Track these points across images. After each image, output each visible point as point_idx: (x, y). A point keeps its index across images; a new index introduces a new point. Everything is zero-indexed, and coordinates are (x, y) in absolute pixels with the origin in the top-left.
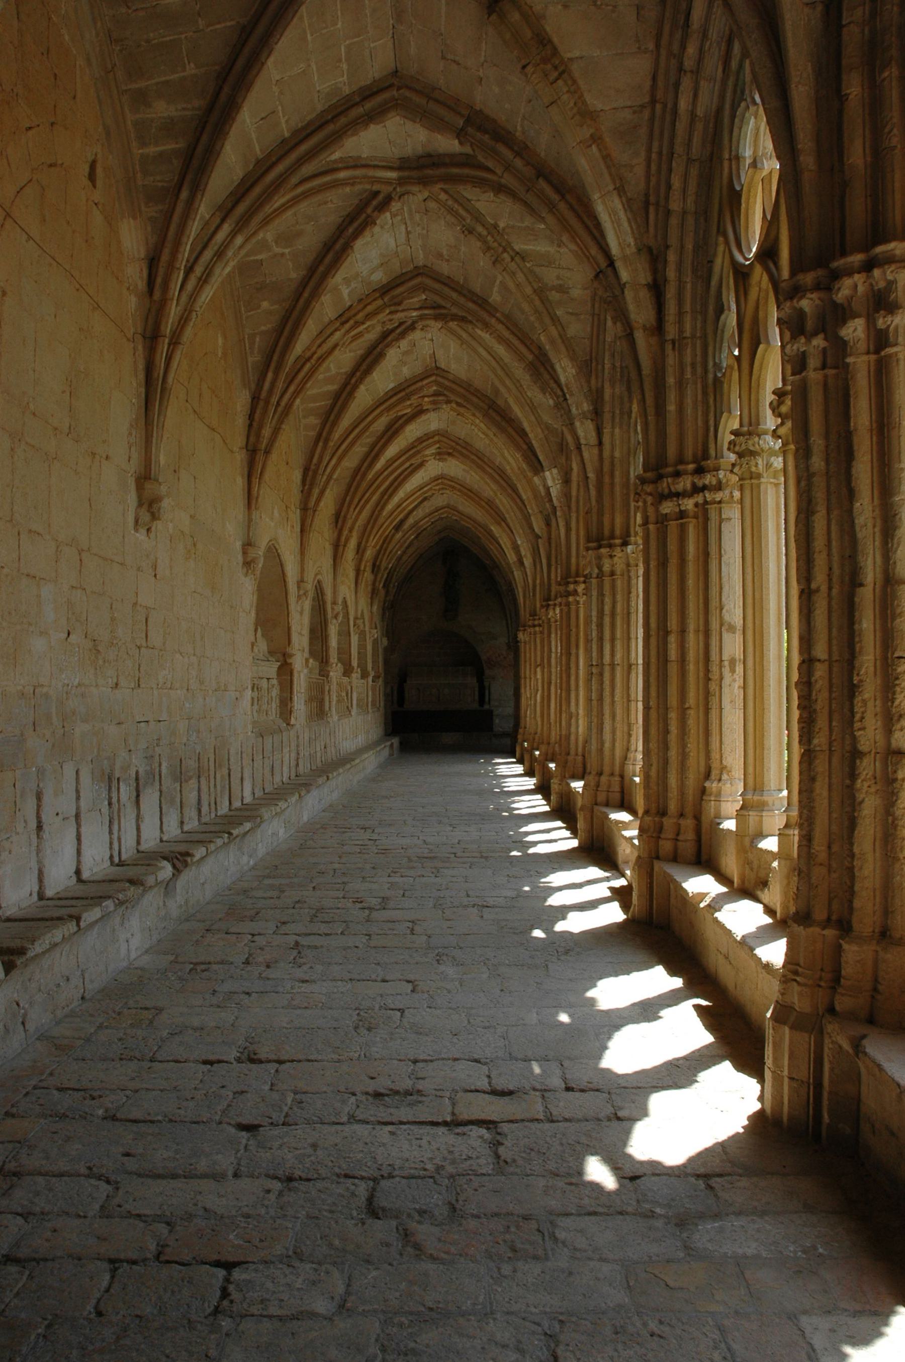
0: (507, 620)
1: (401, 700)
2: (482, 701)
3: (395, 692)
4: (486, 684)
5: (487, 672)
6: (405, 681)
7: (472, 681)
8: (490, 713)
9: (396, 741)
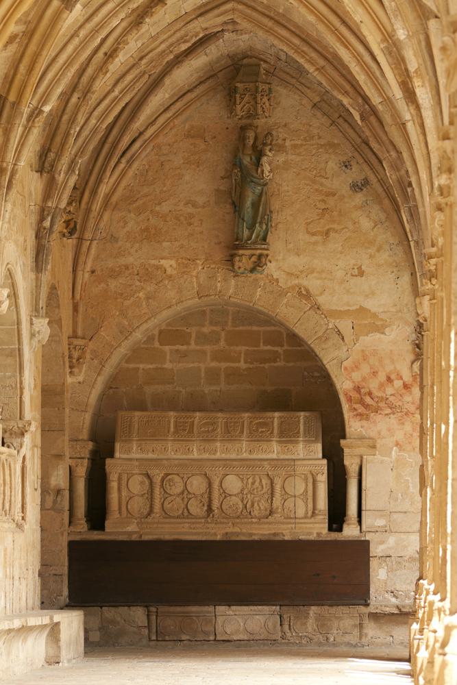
1: (97, 513)
2: (337, 517)
4: (351, 463)
5: (353, 426)
6: (112, 456)
8: (361, 549)
9: (71, 623)
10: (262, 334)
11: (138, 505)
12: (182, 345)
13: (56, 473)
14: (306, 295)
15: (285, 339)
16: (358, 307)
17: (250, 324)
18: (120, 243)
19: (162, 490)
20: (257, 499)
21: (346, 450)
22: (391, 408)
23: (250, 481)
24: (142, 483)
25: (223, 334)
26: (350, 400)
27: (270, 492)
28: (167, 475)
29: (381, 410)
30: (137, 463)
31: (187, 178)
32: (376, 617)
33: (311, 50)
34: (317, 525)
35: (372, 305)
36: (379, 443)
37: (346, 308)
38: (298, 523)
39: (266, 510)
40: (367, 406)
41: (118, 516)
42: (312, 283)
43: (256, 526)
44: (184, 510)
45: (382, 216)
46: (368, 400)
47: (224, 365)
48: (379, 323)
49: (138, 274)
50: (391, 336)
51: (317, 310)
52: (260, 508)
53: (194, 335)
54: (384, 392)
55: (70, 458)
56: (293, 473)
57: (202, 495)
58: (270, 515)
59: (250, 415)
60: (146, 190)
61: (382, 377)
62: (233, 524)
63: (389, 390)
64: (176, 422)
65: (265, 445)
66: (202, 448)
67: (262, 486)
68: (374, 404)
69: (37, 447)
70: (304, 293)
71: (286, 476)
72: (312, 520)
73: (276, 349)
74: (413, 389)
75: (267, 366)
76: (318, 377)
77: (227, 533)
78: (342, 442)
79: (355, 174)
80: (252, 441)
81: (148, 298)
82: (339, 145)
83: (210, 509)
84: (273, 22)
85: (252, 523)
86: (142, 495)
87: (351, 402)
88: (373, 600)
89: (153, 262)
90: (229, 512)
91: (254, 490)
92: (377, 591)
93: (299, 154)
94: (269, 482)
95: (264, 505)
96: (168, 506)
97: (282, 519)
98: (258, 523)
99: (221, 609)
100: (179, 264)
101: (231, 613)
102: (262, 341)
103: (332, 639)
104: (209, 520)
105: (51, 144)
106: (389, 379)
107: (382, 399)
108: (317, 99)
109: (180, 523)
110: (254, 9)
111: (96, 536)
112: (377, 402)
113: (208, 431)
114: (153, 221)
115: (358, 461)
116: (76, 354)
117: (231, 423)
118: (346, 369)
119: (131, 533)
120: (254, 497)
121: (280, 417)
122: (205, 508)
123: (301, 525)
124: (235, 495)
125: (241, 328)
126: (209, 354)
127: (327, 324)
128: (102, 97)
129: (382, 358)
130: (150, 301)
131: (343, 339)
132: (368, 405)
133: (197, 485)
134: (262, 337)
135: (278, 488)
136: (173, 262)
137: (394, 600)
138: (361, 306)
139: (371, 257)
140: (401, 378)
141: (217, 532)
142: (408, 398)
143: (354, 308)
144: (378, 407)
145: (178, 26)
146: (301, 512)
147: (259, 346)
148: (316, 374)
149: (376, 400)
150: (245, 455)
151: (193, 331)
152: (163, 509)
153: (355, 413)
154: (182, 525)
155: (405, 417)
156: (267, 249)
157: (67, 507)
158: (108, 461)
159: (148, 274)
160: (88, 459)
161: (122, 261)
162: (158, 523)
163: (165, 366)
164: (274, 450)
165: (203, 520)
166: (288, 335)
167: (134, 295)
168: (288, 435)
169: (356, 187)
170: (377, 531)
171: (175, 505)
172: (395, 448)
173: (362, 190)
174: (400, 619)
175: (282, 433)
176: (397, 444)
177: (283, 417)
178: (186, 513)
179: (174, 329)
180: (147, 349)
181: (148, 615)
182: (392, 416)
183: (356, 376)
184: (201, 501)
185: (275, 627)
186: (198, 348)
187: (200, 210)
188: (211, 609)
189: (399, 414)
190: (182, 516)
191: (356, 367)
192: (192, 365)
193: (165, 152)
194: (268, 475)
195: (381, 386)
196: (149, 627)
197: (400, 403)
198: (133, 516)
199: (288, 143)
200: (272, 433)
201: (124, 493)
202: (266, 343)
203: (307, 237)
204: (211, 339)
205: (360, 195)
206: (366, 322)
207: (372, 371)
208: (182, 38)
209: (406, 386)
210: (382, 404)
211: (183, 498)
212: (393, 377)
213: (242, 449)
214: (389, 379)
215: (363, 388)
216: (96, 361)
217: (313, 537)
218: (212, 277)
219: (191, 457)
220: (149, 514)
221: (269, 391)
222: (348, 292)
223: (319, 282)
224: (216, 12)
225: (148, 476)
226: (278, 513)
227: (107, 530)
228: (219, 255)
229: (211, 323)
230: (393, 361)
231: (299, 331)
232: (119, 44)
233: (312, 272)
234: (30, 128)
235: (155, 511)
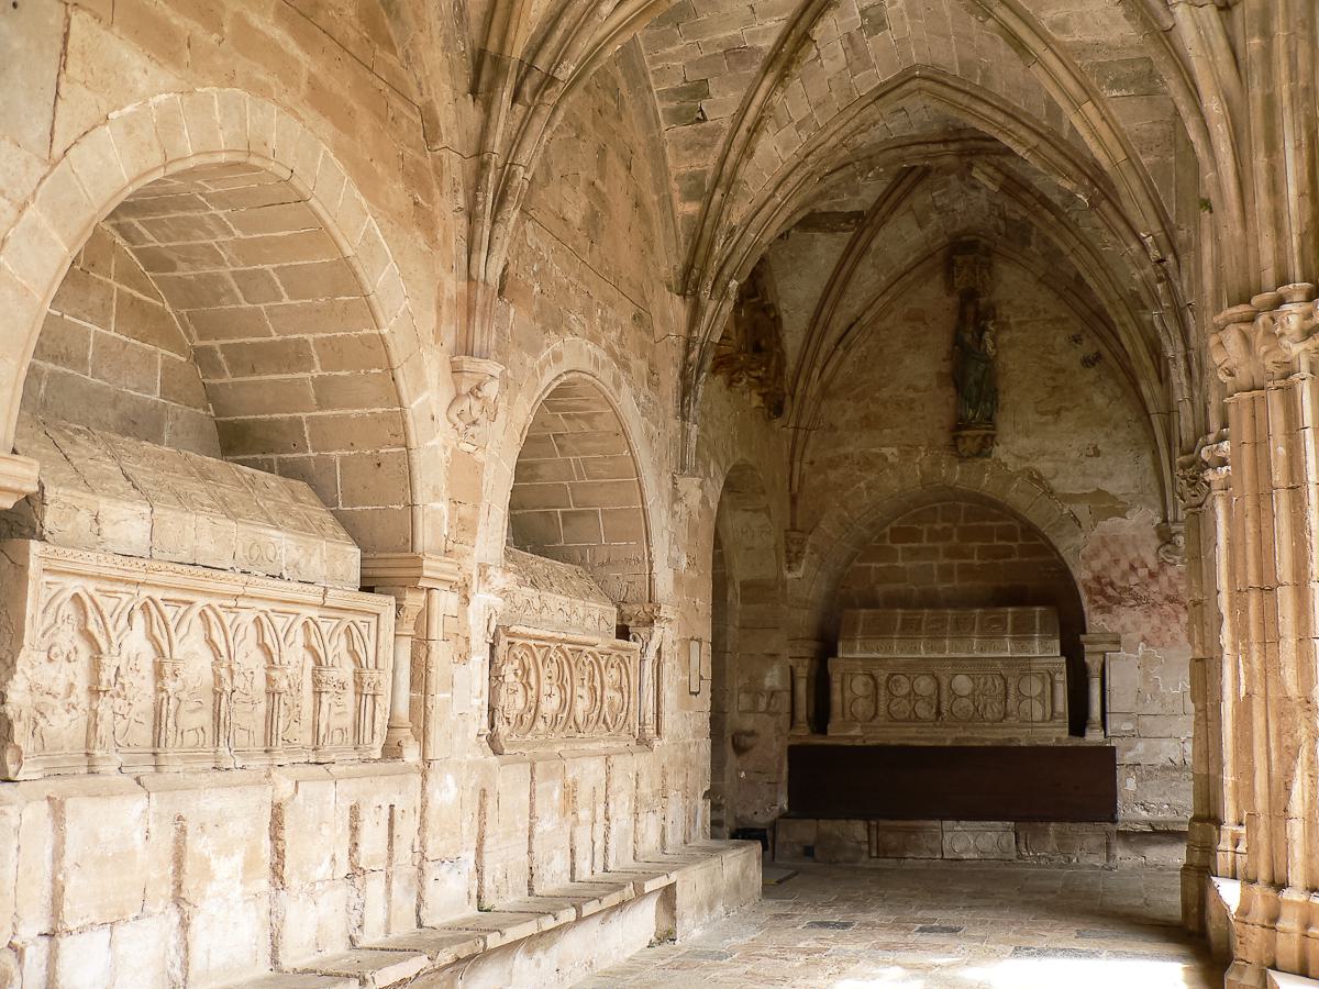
0: (1155, 453)
1: (821, 715)
2: (1079, 722)
3: (802, 687)
4: (1093, 663)
5: (1096, 621)
6: (834, 654)
7: (1046, 652)
8: (1105, 758)
9: (740, 864)
11: (861, 707)
13: (770, 674)
14: (1037, 479)
16: (1095, 490)
18: (839, 432)
20: (989, 700)
23: (982, 680)
24: (866, 684)
25: (955, 530)
26: (1089, 591)
30: (860, 663)
31: (907, 361)
32: (1126, 836)
33: (1020, 126)
34: (1057, 730)
35: (1109, 487)
36: (1124, 638)
39: (1000, 713)
40: (1109, 598)
41: (841, 719)
42: (1044, 466)
43: (988, 730)
45: (1118, 391)
46: (1110, 591)
47: (956, 562)
49: (858, 464)
55: (791, 658)
57: (930, 696)
58: (1004, 717)
59: (982, 610)
60: (865, 377)
61: (1124, 565)
63: (1133, 580)
64: (903, 620)
65: (996, 642)
69: (700, 641)
70: (1035, 476)
72: (1051, 724)
73: (1011, 544)
75: (1001, 561)
77: (957, 738)
78: (1082, 637)
79: (1087, 348)
81: (869, 488)
82: (1067, 319)
83: (939, 712)
84: (968, 96)
86: (867, 697)
88: (1120, 815)
89: (874, 450)
92: (1125, 803)
93: (1025, 331)
95: (997, 707)
99: (948, 824)
100: (900, 451)
101: (959, 828)
103: (1074, 861)
104: (938, 724)
105: (694, 259)
106: (1133, 568)
107: (1125, 589)
108: (1041, 274)
110: (945, 84)
111: (818, 740)
113: (937, 629)
114: (873, 408)
115: (1101, 657)
116: (794, 548)
119: (856, 737)
122: (934, 710)
127: (1061, 510)
128: (761, 204)
131: (1080, 525)
133: (924, 685)
135: (1012, 691)
136: (895, 450)
137: (1144, 813)
138: (1098, 489)
139: (1108, 435)
141: (947, 737)
142: (1154, 588)
143: (1091, 490)
145: (851, 113)
146: (1038, 715)
148: (1053, 569)
150: (977, 654)
151: (925, 528)
156: (993, 429)
157: (787, 708)
158: (830, 661)
159: (869, 463)
160: (812, 659)
161: (841, 451)
162: (883, 727)
163: (896, 564)
164: (1008, 649)
166: (1023, 530)
168: (1022, 631)
169: (1088, 362)
171: (901, 708)
173: (1094, 364)
174: (1154, 837)
175: (1016, 629)
176: (1144, 639)
178: (913, 717)
181: (868, 830)
183: (1096, 565)
185: (1009, 846)
186: (931, 545)
187: (920, 394)
188: (936, 823)
191: (1096, 555)
193: (884, 337)
195: (1124, 576)
196: (869, 842)
197: (1146, 594)
198: (856, 720)
199: (1012, 321)
201: (848, 694)
202: (1001, 538)
203: (1036, 416)
204: (945, 535)
205: (1092, 370)
208: (857, 128)
209: (1152, 575)
210: (1125, 596)
213: (974, 648)
214: (1133, 568)
215: (1104, 577)
216: (815, 556)
217: (1052, 742)
218: (936, 463)
219: (919, 656)
220: (874, 717)
222: (1084, 474)
223: (1050, 465)
224: (898, 91)
225: (872, 677)
226: (1012, 716)
227: (830, 734)
228: (943, 439)
230: (1136, 549)
231: (1033, 517)
232: (763, 111)
233: (1044, 455)
234: (536, 108)
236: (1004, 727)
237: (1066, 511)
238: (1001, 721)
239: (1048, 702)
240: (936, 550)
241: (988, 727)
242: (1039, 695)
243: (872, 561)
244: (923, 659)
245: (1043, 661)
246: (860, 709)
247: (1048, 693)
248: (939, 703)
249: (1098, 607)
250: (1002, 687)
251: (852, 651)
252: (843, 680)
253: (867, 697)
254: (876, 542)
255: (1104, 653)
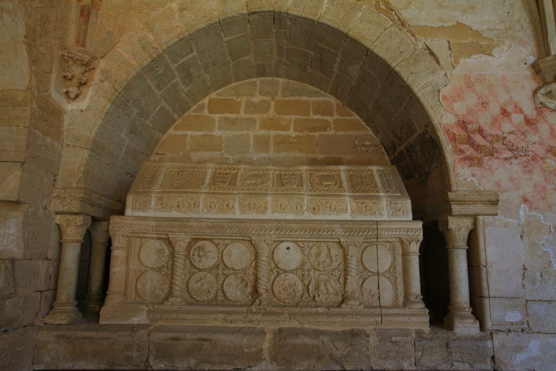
6: (121, 213)
10: (311, 104)
12: (232, 113)
15: (335, 109)
16: (455, 23)
17: (300, 95)
19: (188, 262)
21: (456, 208)
22: (511, 150)
23: (314, 251)
25: (273, 103)
26: (453, 138)
27: (342, 267)
28: (196, 240)
29: (498, 152)
30: (154, 224)
34: (415, 319)
36: (502, 197)
37: (439, 24)
38: (387, 315)
39: (336, 294)
40: (477, 148)
43: (324, 319)
44: (217, 292)
46: (478, 139)
48: (484, 43)
50: (502, 58)
51: (401, 27)
52: (327, 290)
53: (243, 105)
54: (500, 129)
56: (375, 240)
57: (245, 270)
61: (495, 109)
62: (290, 315)
63: (507, 127)
65: (333, 202)
66: (247, 203)
67: (331, 259)
68: (488, 145)
71: (365, 245)
72: (406, 311)
73: (326, 118)
74: (539, 125)
75: (317, 134)
76: (370, 145)
80: (315, 195)
81: (182, 9)
85: (318, 314)
86: (159, 270)
87: (455, 141)
90: (284, 296)
91: (319, 264)
94: (340, 253)
95: (334, 286)
96: (195, 286)
97: (361, 308)
98: (327, 315)
102: (312, 111)
104: (254, 308)
106: (505, 113)
107: (497, 138)
109: (211, 313)
112: (491, 142)
115: (467, 223)
117: (285, 175)
118: (445, 98)
120: (320, 275)
121: (346, 170)
122: (249, 290)
123: (390, 318)
124: (292, 272)
125: (291, 98)
126: (258, 122)
129: (492, 85)
130: (185, 12)
131: (438, 62)
132: (479, 146)
134: (311, 107)
135: (353, 262)
138: (458, 22)
140: (521, 112)
142: (533, 138)
143: (450, 24)
144: (493, 148)
146: (387, 298)
147: (309, 115)
148: (367, 143)
149: (489, 139)
150: (307, 216)
151: (243, 100)
152: (188, 290)
153: (462, 156)
154: (214, 316)
155: (532, 162)
165: (245, 309)
167: (164, 5)
170: (509, 331)
172: (522, 205)
176: (525, 200)
177: (351, 170)
178: (220, 298)
179: (224, 98)
180: (196, 116)
182: (513, 161)
183: (460, 107)
184: (244, 280)
186: (248, 116)
189: (524, 159)
190: (213, 302)
191: (459, 96)
192: (240, 133)
194: (339, 243)
195: (495, 121)
197: (524, 144)
200: (341, 186)
201: (134, 266)
202: (316, 112)
206: (467, 41)
207: (481, 101)
209: (528, 121)
210: (498, 146)
211: (218, 274)
212: (510, 109)
216: (106, 84)
219: (231, 216)
220: (166, 299)
221: (319, 159)
225: (169, 243)
226: (354, 299)
227: (102, 322)
229: (261, 93)
235: (175, 293)
236: (345, 315)
237: (420, 45)
238: (339, 306)
239: (400, 280)
240: (253, 121)
241: (323, 314)
242: (389, 271)
243: (189, 129)
244: (235, 221)
245: (392, 226)
246: (148, 285)
247: (399, 269)
248: (256, 279)
249: (465, 159)
250: (340, 260)
251: (144, 207)
252: (129, 247)
253: (159, 270)
254: (193, 111)
255: (475, 217)
